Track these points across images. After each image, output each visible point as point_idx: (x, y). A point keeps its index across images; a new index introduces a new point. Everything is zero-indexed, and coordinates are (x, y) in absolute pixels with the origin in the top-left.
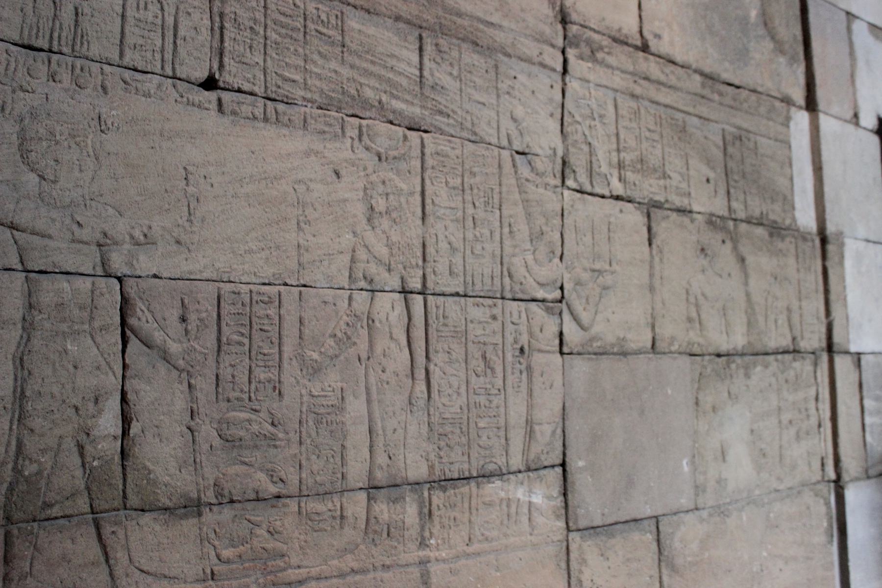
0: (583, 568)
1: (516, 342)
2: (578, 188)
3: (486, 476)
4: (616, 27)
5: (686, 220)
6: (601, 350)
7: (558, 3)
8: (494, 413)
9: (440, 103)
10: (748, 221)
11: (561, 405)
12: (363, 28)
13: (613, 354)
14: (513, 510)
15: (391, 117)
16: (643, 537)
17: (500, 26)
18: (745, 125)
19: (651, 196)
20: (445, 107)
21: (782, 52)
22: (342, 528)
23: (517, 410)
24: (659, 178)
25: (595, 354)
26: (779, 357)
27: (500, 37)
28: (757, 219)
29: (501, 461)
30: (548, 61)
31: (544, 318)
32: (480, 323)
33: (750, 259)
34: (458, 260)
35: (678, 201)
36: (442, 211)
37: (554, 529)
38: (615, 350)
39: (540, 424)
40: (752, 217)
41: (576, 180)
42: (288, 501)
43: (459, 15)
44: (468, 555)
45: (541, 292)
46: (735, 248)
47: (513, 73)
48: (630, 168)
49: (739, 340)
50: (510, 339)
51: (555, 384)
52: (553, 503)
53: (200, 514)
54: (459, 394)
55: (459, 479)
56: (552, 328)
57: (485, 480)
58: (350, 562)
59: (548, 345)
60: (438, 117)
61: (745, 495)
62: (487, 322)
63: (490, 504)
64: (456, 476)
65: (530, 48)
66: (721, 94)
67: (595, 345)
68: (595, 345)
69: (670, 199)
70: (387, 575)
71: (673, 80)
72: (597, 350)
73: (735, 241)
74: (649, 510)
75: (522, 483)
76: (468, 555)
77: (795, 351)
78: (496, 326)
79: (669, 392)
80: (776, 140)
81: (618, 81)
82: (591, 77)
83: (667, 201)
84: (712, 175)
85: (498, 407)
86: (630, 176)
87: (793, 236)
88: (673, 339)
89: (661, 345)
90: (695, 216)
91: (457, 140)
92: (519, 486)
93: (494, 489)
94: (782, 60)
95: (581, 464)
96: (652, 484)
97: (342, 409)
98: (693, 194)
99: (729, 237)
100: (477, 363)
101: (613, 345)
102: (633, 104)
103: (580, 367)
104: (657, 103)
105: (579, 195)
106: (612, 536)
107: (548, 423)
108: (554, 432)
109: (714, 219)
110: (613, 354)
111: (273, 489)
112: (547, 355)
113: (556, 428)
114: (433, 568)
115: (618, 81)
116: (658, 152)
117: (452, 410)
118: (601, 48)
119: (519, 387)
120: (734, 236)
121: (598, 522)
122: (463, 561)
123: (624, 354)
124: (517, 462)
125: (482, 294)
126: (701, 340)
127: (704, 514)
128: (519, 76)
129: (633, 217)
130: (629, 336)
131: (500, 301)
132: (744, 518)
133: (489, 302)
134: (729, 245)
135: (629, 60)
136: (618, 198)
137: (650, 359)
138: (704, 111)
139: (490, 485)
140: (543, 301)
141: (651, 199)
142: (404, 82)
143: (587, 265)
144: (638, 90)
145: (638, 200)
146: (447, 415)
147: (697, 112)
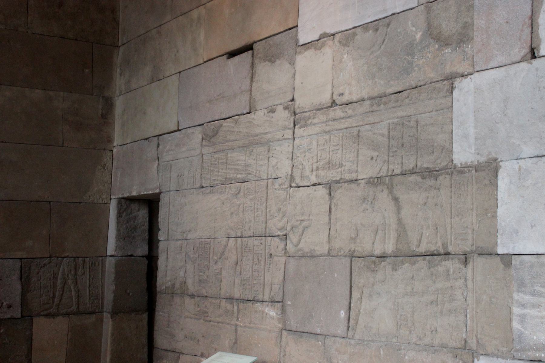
0: (287, 346)
1: (269, 253)
2: (296, 186)
3: (254, 301)
4: (318, 103)
5: (353, 186)
6: (302, 255)
7: (292, 109)
8: (259, 279)
9: (250, 171)
10: (402, 174)
11: (283, 278)
12: (231, 155)
13: (307, 257)
14: (264, 314)
15: (238, 181)
16: (317, 343)
17: (270, 132)
18: (404, 114)
19: (332, 179)
20: (251, 171)
21: (447, 45)
22: (219, 309)
23: (268, 278)
24: (338, 168)
25: (299, 257)
26: (428, 258)
27: (269, 136)
28: (409, 170)
29: (260, 297)
30: (286, 136)
31: (278, 242)
32: (257, 246)
33: (403, 197)
34: (252, 224)
35: (347, 177)
36: (248, 208)
37: (277, 326)
38: (309, 255)
39: (274, 284)
40: (406, 171)
41: (295, 183)
42: (209, 298)
43: (257, 135)
44: (249, 328)
45: (279, 232)
46: (391, 192)
47: (274, 148)
48: (321, 169)
49: (390, 248)
50: (267, 251)
51: (281, 270)
52: (278, 316)
53: (194, 298)
54: (249, 271)
55: (247, 300)
56: (282, 246)
57: (255, 302)
58: (220, 320)
59: (280, 253)
60: (249, 176)
61: (384, 339)
62: (259, 246)
63: (256, 311)
64: (246, 299)
65: (279, 135)
66: (385, 103)
67: (299, 253)
68: (299, 253)
69: (343, 177)
70: (227, 326)
71: (350, 112)
72: (300, 255)
73: (391, 189)
74: (319, 331)
75: (268, 306)
76: (249, 328)
77: (447, 254)
78: (262, 247)
79: (336, 275)
80: (437, 111)
81: (317, 129)
82: (305, 134)
83: (341, 178)
84: (375, 154)
85: (261, 277)
86: (321, 173)
87: (447, 173)
88: (341, 249)
89: (333, 253)
90: (359, 181)
91: (253, 182)
92: (266, 307)
93: (258, 305)
94: (448, 50)
95: (289, 303)
96: (322, 319)
97: (221, 274)
98: (359, 170)
99: (386, 186)
100: (256, 261)
101: (307, 253)
102: (327, 137)
103: (292, 263)
104: (341, 129)
105: (297, 189)
106: (301, 337)
107: (278, 284)
108: (279, 288)
109: (371, 180)
110: (307, 257)
111: (206, 294)
112: (279, 258)
113: (280, 287)
114: (239, 328)
115: (317, 129)
116: (339, 155)
117: (247, 276)
118: (309, 118)
119: (269, 269)
120: (390, 186)
121: (294, 329)
122: (247, 329)
123: (313, 257)
124: (266, 298)
125: (258, 236)
126: (360, 249)
127: (353, 342)
128: (276, 148)
129: (322, 191)
130: (316, 248)
131: (264, 238)
132: (382, 353)
133: (260, 238)
134: (386, 192)
135: (324, 116)
136: (314, 185)
137: (326, 259)
138: (371, 119)
139: (256, 304)
140: (278, 236)
141: (332, 180)
142: (240, 167)
143: (298, 218)
144: (328, 128)
145: (324, 183)
146: (245, 278)
147: (366, 123)
